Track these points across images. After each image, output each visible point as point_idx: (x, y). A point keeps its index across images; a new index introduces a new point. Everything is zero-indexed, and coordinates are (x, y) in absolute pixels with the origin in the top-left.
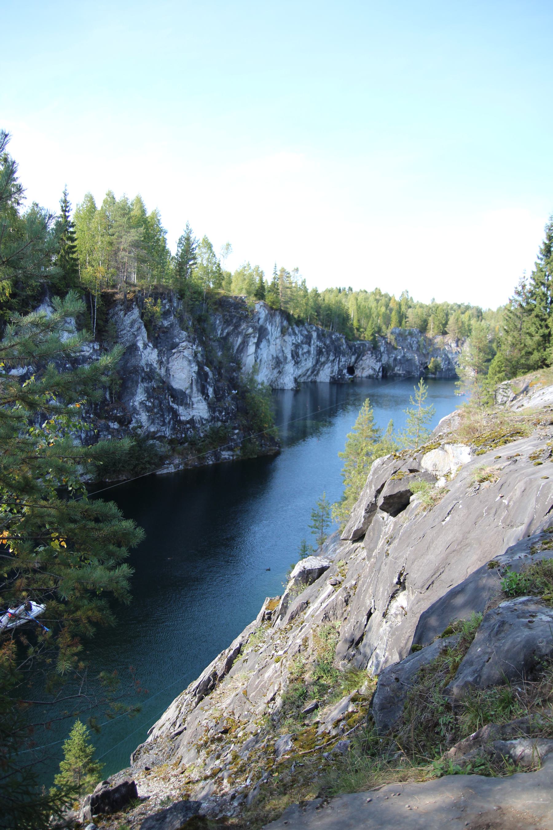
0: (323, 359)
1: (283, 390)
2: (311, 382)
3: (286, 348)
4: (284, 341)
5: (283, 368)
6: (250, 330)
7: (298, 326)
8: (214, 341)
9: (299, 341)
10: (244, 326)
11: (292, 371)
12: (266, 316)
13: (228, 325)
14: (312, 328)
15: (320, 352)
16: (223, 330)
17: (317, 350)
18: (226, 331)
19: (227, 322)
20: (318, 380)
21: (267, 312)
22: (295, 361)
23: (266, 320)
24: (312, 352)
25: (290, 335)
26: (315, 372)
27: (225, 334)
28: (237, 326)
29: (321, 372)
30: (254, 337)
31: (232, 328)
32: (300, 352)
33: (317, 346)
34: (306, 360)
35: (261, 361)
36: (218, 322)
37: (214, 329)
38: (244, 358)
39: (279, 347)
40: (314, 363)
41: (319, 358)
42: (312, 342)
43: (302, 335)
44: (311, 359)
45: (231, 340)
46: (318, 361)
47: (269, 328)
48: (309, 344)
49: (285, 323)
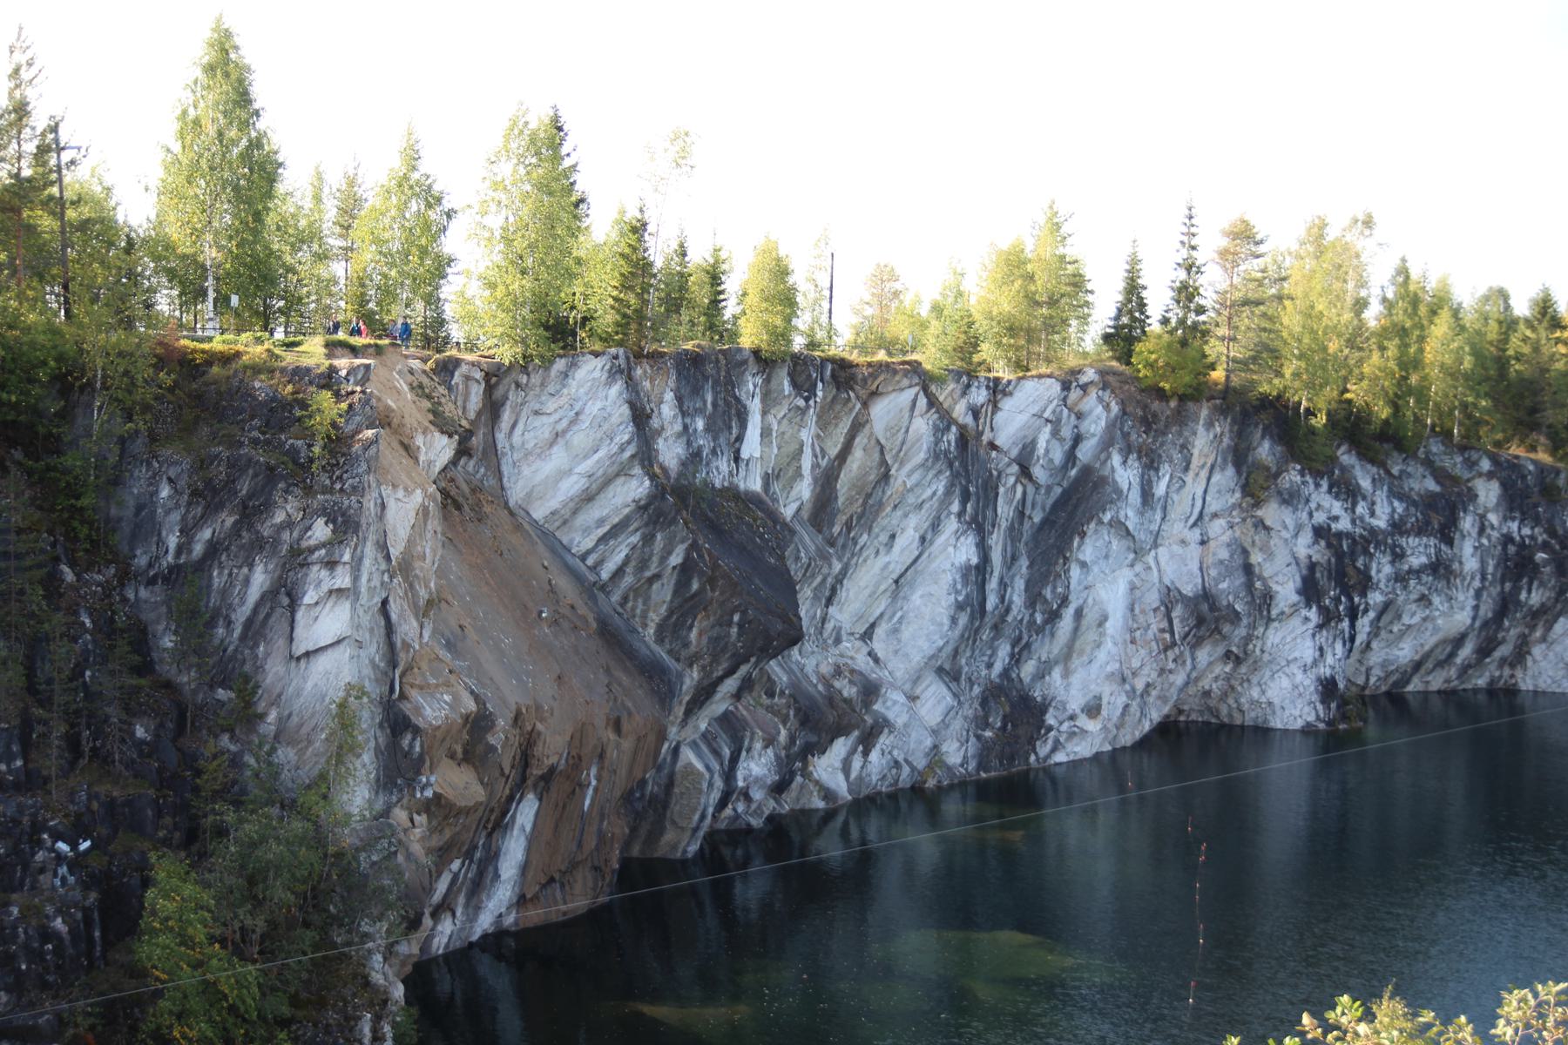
0: (1535, 597)
1: (1262, 733)
2: (1491, 691)
3: (1270, 555)
4: (1261, 525)
5: (1248, 639)
6: (321, 531)
7: (1367, 455)
8: (151, 582)
9: (1381, 523)
10: (286, 509)
11: (1307, 651)
12: (1111, 426)
13: (212, 509)
14: (1471, 464)
15: (1516, 565)
16: (188, 532)
17: (1504, 558)
18: (206, 534)
19: (206, 496)
20: (1526, 683)
21: (1115, 408)
22: (1323, 610)
23: (1106, 444)
24: (1471, 564)
25: (1290, 499)
26: (1504, 651)
27: (198, 549)
28: (252, 512)
29: (1537, 651)
30: (331, 565)
31: (230, 521)
32: (1381, 568)
33: (1507, 539)
34: (1424, 600)
35: (1079, 614)
36: (165, 492)
37: (146, 524)
38: (274, 669)
39: (1224, 554)
40: (1487, 610)
41: (1516, 590)
42: (1468, 523)
43: (1396, 494)
44: (1465, 598)
45: (218, 579)
46: (1506, 606)
47: (1125, 474)
48: (1447, 533)
49: (1265, 451)
